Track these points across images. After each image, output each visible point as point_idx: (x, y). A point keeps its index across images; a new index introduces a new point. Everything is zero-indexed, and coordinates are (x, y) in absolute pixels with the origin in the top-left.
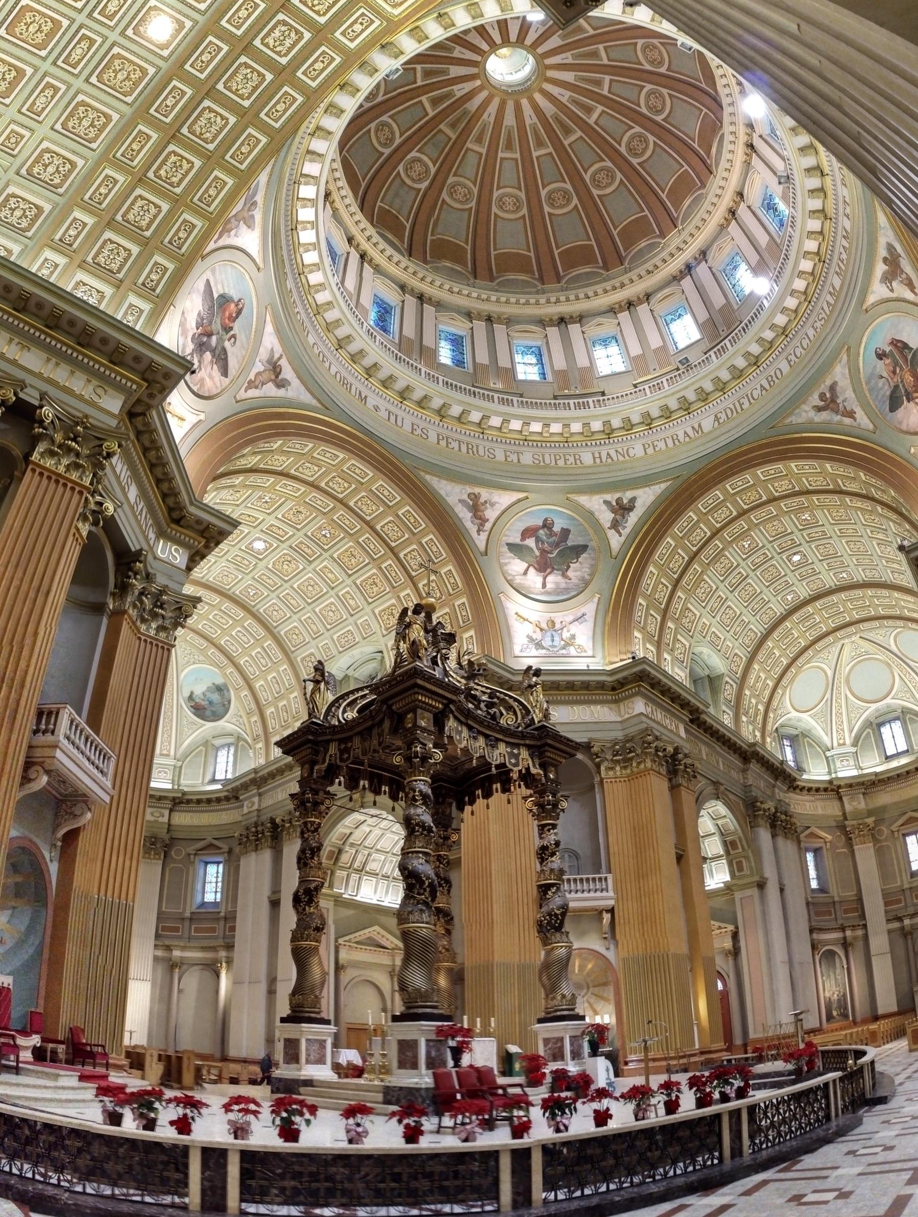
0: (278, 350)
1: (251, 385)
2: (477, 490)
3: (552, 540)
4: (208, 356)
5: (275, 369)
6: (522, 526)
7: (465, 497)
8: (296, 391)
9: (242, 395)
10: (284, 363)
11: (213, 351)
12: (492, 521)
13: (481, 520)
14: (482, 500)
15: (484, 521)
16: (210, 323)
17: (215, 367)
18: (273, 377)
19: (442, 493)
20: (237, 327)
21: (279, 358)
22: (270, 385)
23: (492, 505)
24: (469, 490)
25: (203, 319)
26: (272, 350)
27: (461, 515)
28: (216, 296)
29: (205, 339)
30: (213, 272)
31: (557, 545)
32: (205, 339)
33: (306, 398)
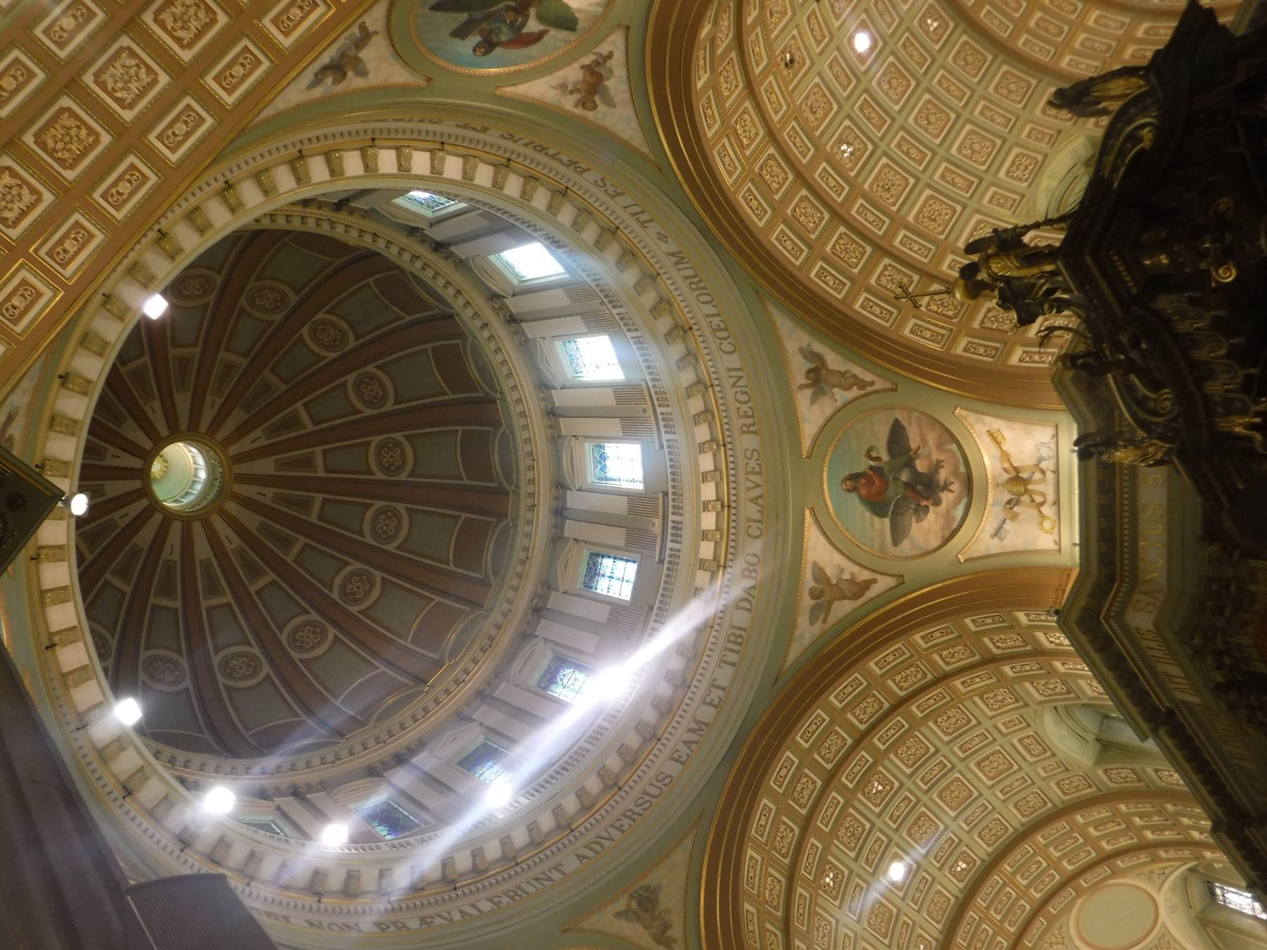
0: (803, 399)
1: (862, 384)
2: (579, 111)
3: (492, 26)
4: (921, 466)
5: (818, 378)
6: (533, 50)
7: (602, 108)
9: (879, 384)
10: (800, 379)
11: (910, 464)
12: (577, 65)
14: (576, 97)
15: (590, 69)
16: (904, 498)
17: (913, 445)
18: (823, 372)
19: (635, 124)
20: (863, 465)
24: (590, 115)
25: (916, 511)
26: (814, 400)
27: (624, 87)
28: (887, 521)
29: (919, 487)
30: (883, 547)
31: (488, 17)
32: (919, 487)
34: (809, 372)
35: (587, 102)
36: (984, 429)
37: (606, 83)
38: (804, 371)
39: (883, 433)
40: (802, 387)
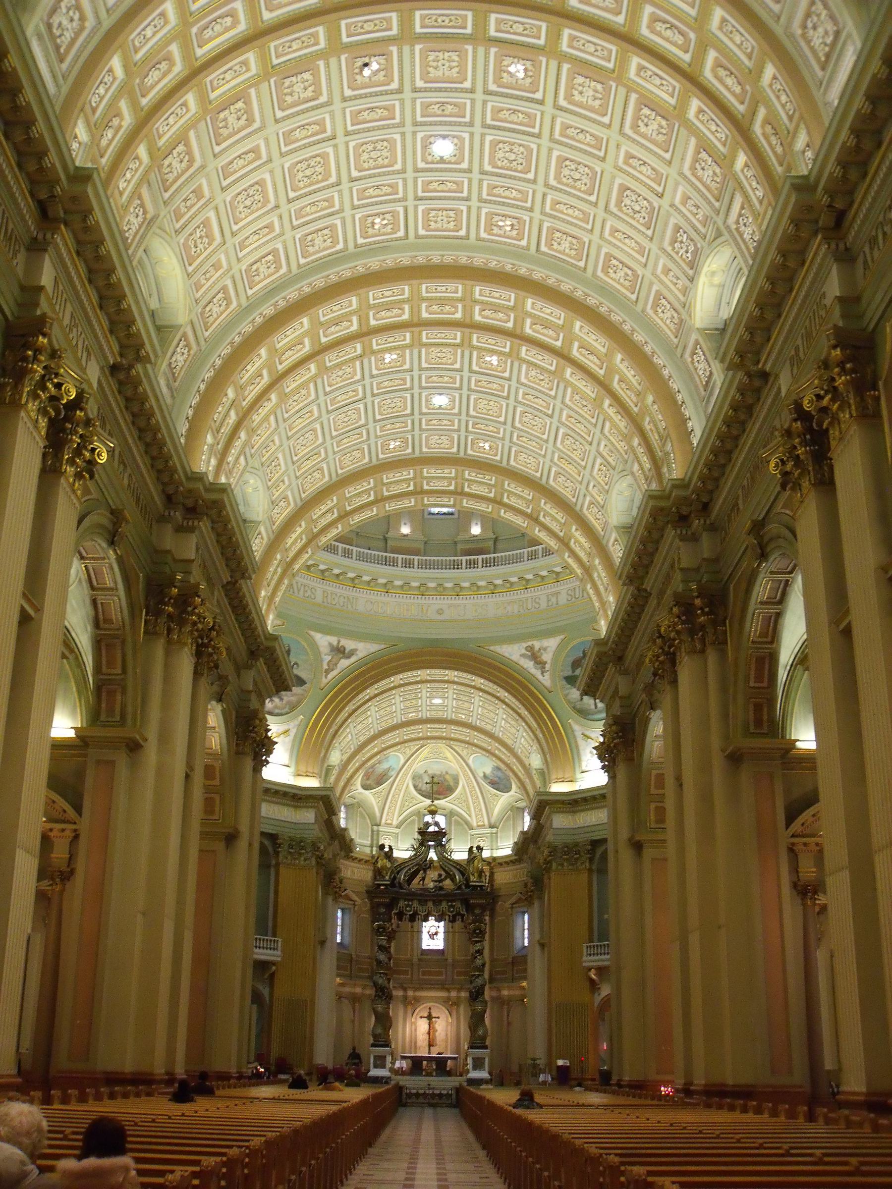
0: (334, 640)
1: (327, 672)
5: (340, 651)
7: (524, 651)
8: (363, 649)
9: (325, 681)
12: (549, 662)
13: (541, 664)
14: (537, 648)
19: (506, 655)
20: (293, 659)
21: (339, 642)
22: (342, 661)
23: (545, 649)
24: (525, 645)
26: (330, 644)
27: (525, 666)
33: (373, 647)
34: (345, 649)
35: (530, 649)
36: (290, 727)
37: (532, 663)
38: (346, 646)
39: (303, 675)
40: (339, 642)
